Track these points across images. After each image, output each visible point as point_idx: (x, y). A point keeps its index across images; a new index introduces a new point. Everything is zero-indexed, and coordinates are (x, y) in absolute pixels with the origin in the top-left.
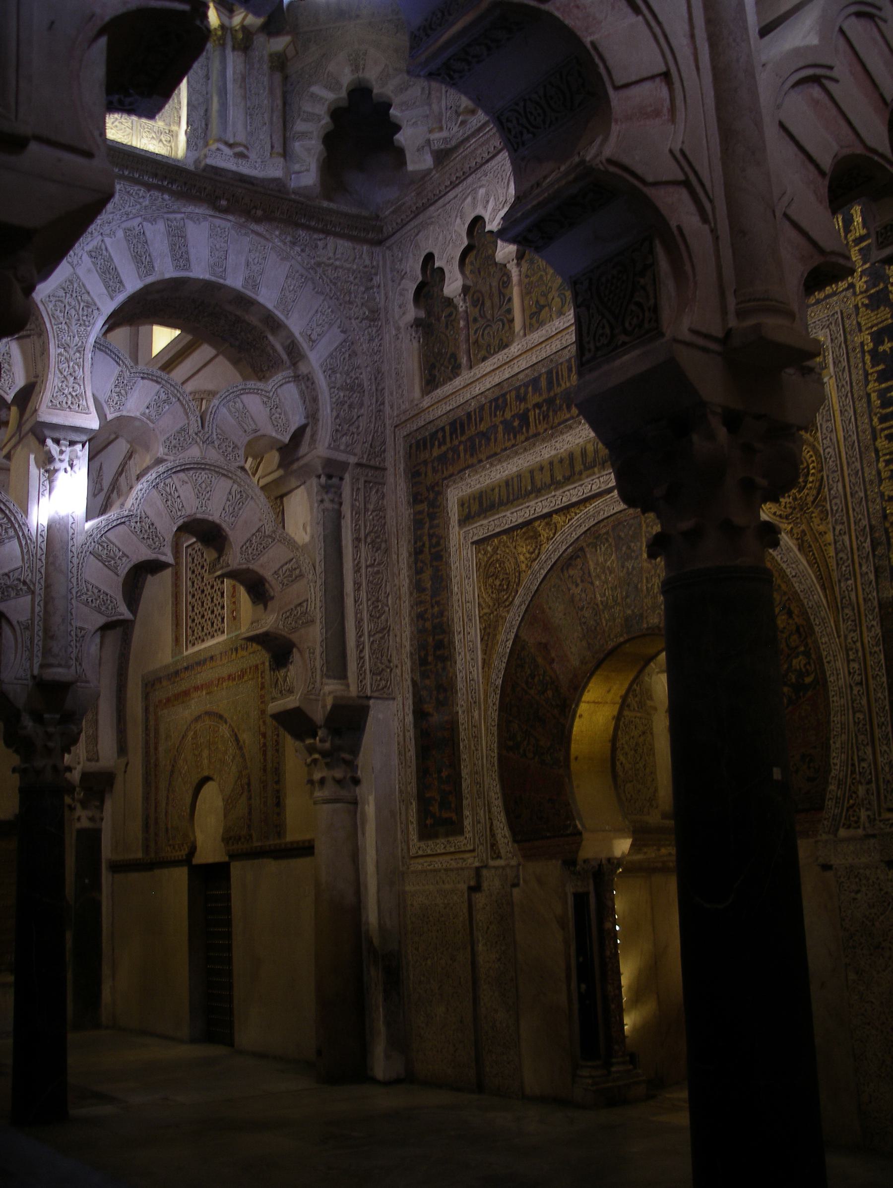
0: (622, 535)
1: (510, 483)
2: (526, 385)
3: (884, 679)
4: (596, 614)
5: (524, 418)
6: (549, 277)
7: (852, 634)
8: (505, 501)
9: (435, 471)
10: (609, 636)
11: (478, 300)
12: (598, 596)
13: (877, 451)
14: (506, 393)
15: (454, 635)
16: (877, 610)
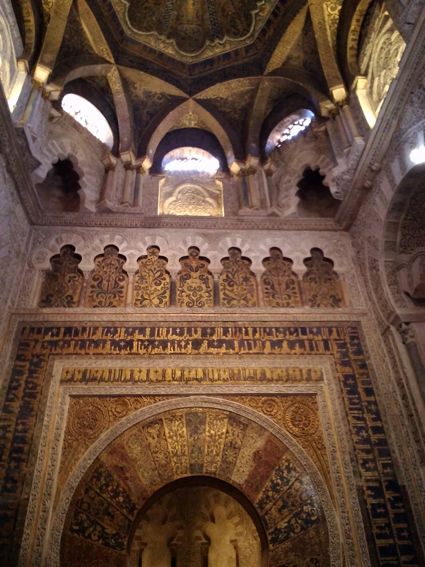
0: (193, 420)
1: (113, 371)
2: (134, 329)
3: (362, 524)
4: (167, 458)
5: (130, 344)
6: (153, 289)
7: (343, 499)
8: (106, 379)
9: (43, 347)
10: (176, 472)
11: (98, 279)
12: (170, 447)
13: (349, 422)
14: (117, 327)
15: (36, 446)
16: (355, 490)
